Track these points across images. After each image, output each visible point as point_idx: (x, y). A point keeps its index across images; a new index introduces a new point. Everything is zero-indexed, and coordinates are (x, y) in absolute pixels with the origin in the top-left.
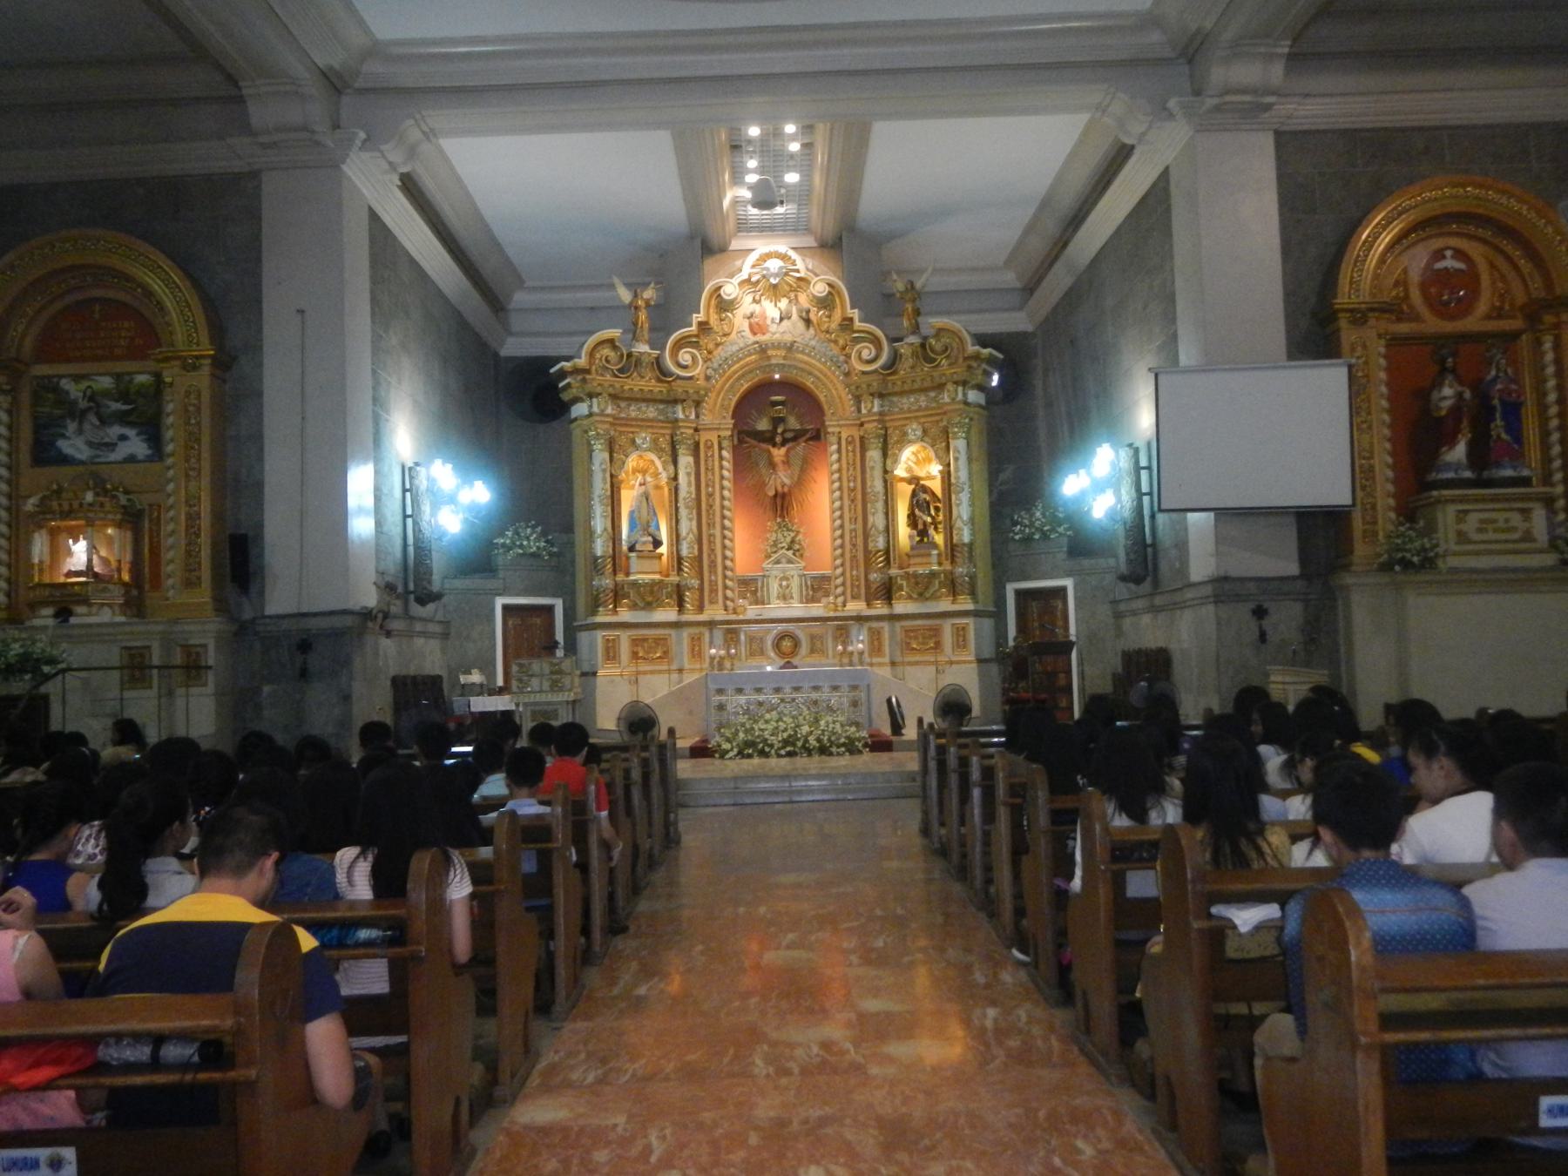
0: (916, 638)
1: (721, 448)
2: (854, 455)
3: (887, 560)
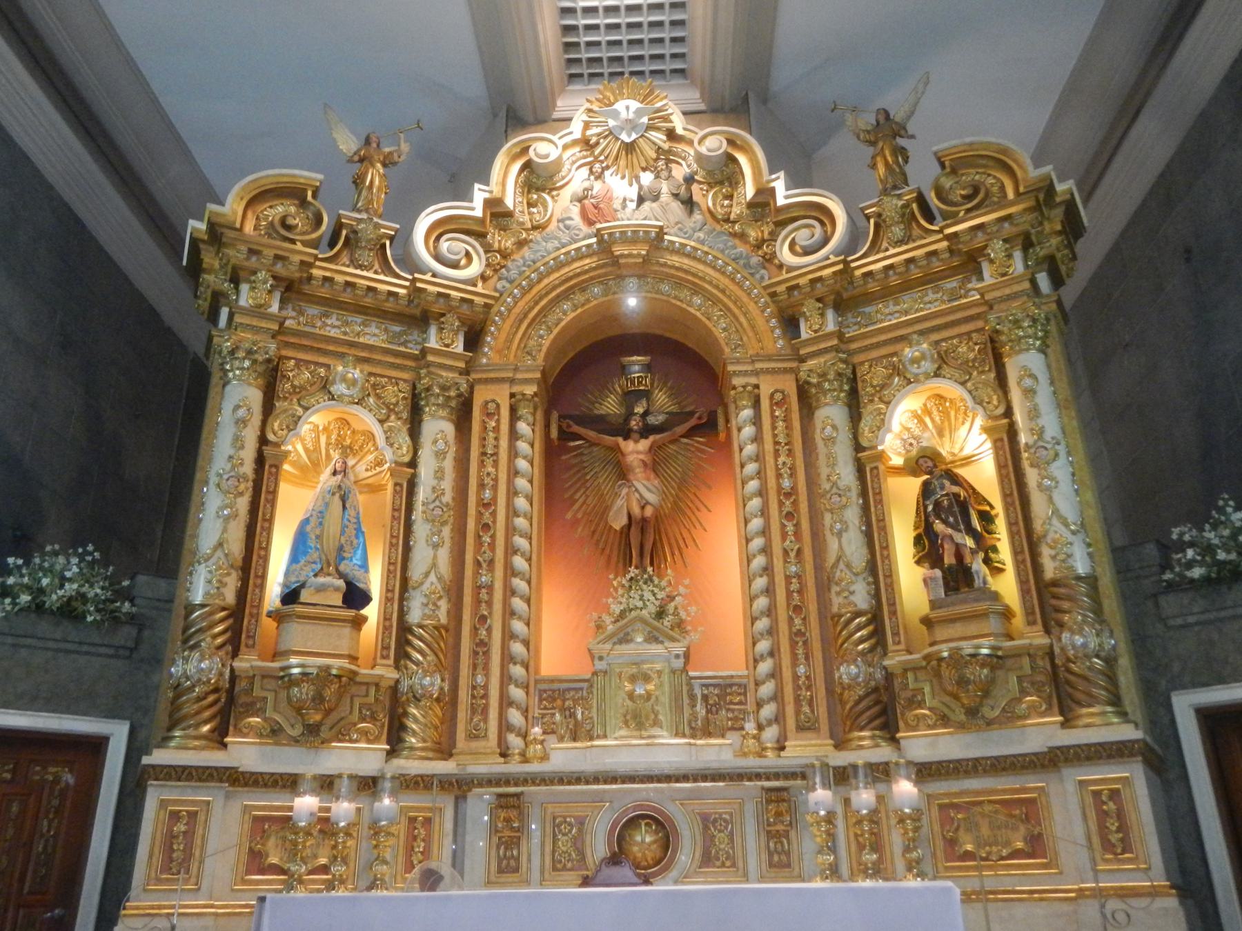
0: (972, 826)
2: (789, 427)
3: (878, 635)
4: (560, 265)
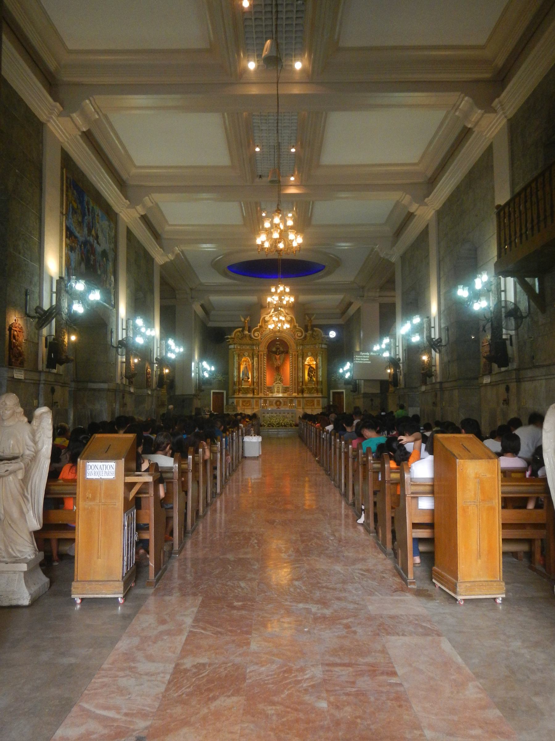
1: (264, 356)
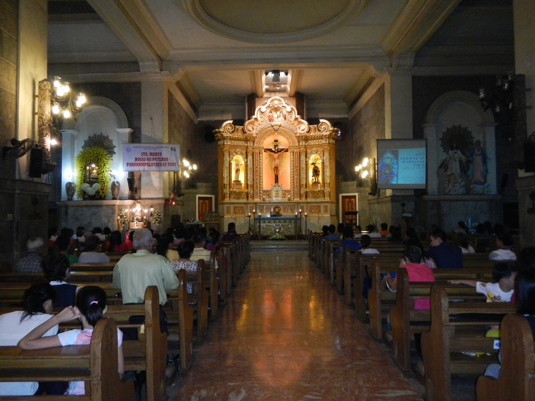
3: (306, 187)
4: (266, 129)
